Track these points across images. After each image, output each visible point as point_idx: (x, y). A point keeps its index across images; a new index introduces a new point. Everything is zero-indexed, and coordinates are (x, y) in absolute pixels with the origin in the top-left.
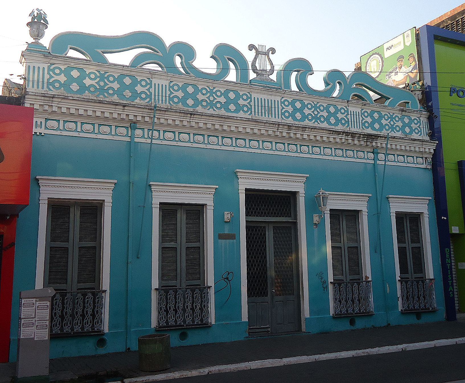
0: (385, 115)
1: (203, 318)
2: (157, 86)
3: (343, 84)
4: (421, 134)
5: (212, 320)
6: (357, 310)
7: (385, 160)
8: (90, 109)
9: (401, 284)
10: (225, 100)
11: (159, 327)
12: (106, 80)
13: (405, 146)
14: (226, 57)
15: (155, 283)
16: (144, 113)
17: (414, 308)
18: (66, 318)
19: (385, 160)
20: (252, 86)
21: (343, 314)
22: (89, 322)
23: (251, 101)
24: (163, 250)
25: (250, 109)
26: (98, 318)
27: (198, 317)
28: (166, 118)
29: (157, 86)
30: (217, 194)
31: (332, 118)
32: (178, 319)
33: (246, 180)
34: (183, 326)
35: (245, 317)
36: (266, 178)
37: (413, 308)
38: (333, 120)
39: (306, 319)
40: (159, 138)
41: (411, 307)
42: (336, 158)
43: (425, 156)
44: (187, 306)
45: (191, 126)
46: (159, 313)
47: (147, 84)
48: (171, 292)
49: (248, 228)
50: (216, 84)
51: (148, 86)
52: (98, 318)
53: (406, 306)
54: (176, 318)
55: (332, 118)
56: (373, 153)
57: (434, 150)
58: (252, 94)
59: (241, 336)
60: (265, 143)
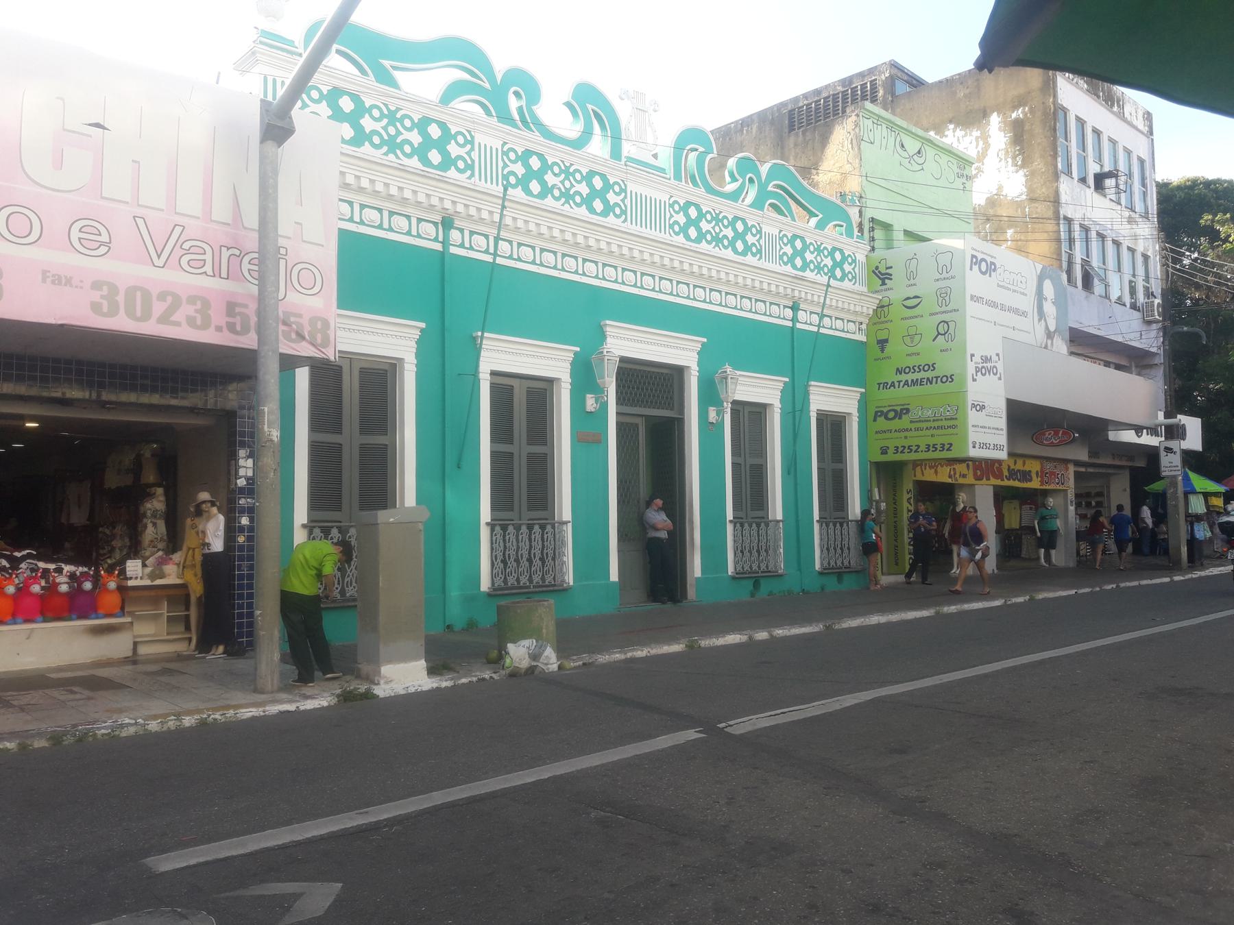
0: (811, 243)
1: (347, 589)
2: (658, 202)
3: (756, 182)
4: (856, 282)
5: (570, 579)
6: (763, 567)
7: (819, 326)
8: (557, 227)
9: (735, 527)
10: (362, 122)
11: (494, 590)
12: (398, 124)
13: (718, 271)
14: (590, 107)
15: (730, 515)
16: (436, 189)
17: (751, 569)
18: (349, 572)
19: (819, 326)
20: (628, 168)
21: (745, 573)
22: (500, 573)
23: (625, 197)
24: (316, 450)
25: (470, 167)
26: (351, 574)
27: (513, 574)
28: (597, 237)
29: (658, 202)
30: (863, 403)
31: (740, 242)
32: (495, 577)
33: (654, 347)
34: (528, 587)
35: (614, 576)
36: (649, 340)
37: (765, 569)
38: (740, 246)
39: (697, 579)
40: (462, 246)
41: (747, 568)
42: (543, 271)
43: (860, 319)
44: (522, 555)
45: (564, 240)
46: (735, 554)
47: (467, 142)
48: (537, 528)
49: (620, 426)
50: (446, 114)
51: (469, 147)
52: (351, 574)
53: (826, 564)
54: (505, 575)
55: (740, 242)
56: (791, 308)
57: (874, 310)
58: (629, 184)
59: (609, 606)
60: (587, 263)
